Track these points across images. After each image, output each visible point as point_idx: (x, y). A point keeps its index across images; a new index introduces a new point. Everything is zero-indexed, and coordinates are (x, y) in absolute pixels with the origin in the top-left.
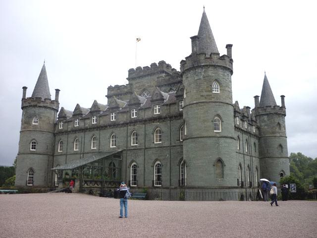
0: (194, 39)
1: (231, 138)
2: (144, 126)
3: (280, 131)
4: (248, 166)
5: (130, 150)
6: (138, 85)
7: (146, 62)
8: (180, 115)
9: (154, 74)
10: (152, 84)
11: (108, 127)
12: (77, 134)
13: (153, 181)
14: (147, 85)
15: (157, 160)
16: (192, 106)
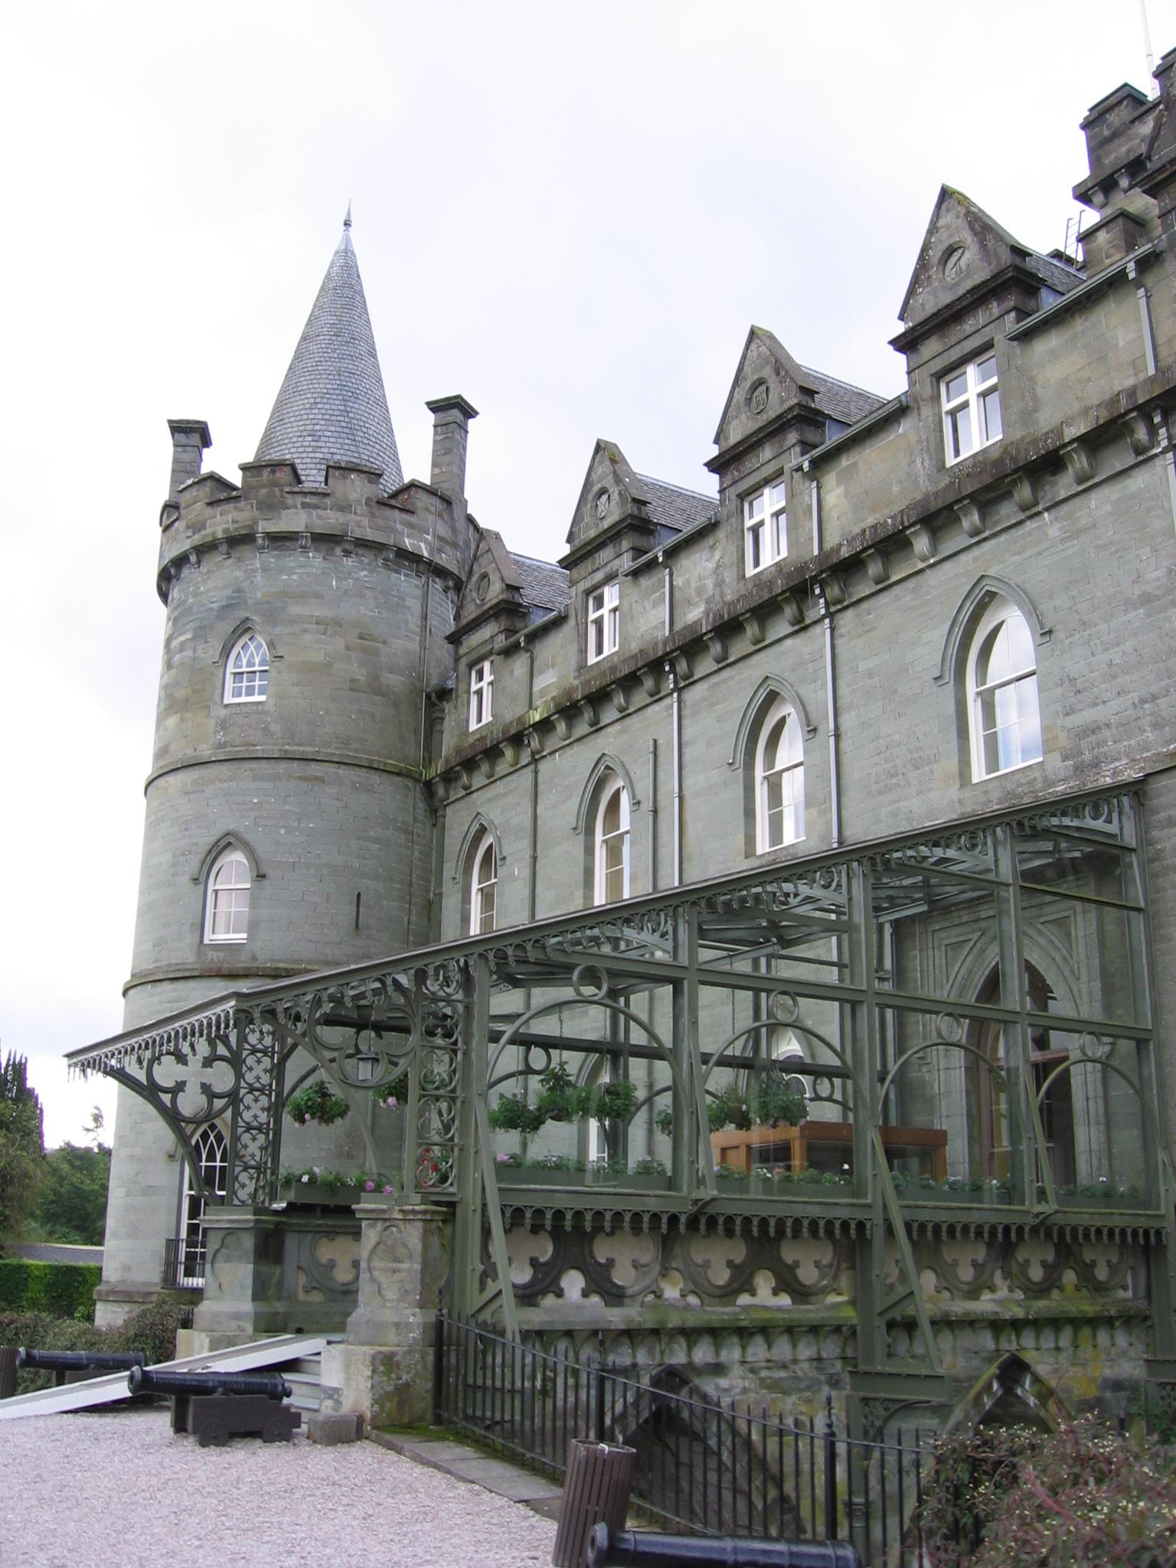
11: (921, 544)
12: (612, 741)
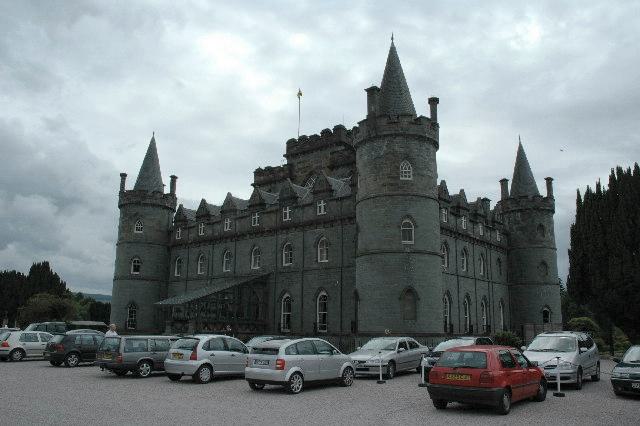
0: (371, 91)
1: (430, 253)
2: (301, 234)
3: (541, 238)
4: (484, 298)
5: (281, 273)
6: (300, 166)
7: (313, 129)
8: (352, 218)
9: (326, 147)
10: (323, 164)
13: (315, 324)
14: (315, 166)
15: (320, 289)
16: (368, 201)
